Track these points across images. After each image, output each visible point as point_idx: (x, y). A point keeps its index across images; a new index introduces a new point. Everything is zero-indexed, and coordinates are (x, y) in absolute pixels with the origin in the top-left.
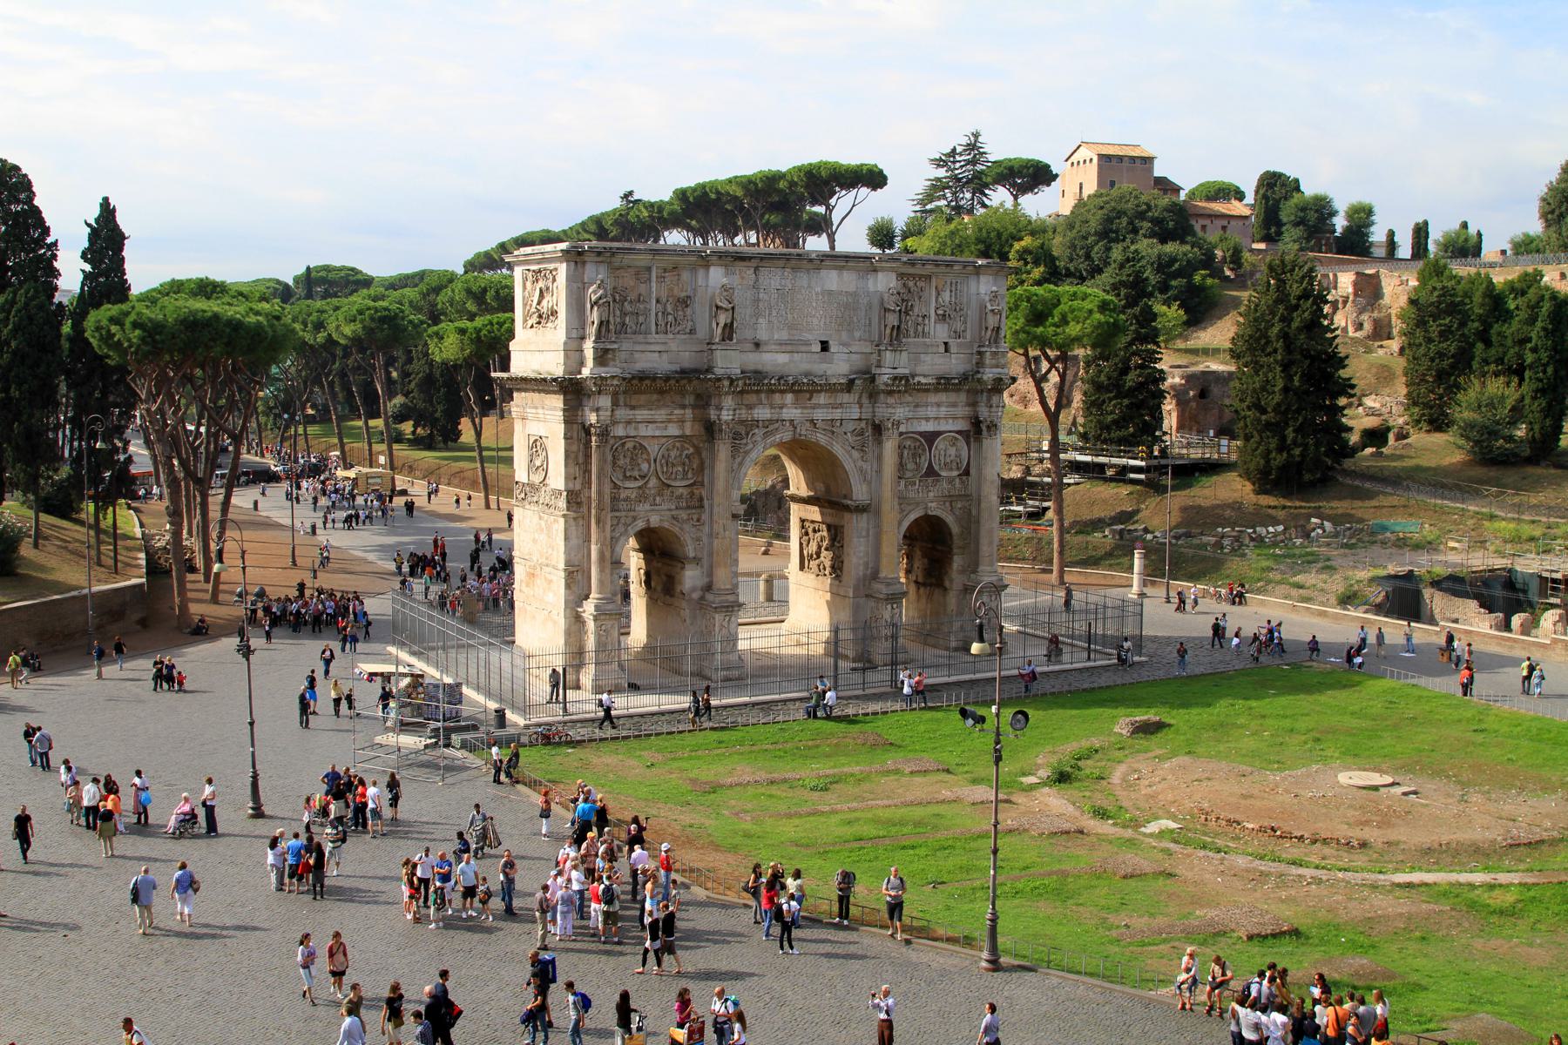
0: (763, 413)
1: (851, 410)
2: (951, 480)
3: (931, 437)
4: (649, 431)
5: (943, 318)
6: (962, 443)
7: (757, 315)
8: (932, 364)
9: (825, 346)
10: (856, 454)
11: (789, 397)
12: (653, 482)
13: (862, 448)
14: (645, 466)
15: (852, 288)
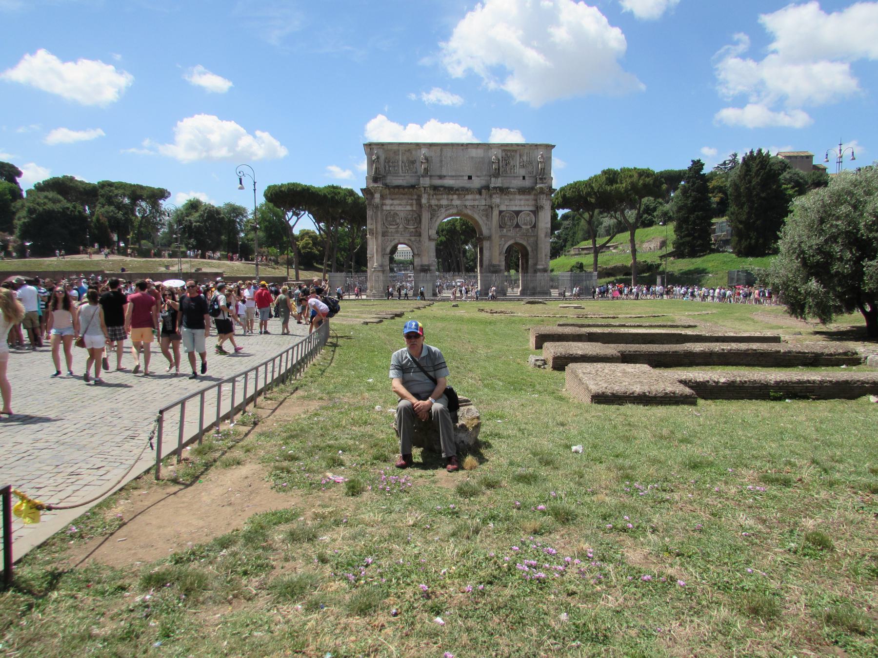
0: (444, 202)
1: (482, 202)
2: (527, 230)
3: (517, 213)
5: (523, 166)
6: (532, 215)
7: (441, 167)
8: (517, 183)
9: (470, 178)
10: (484, 218)
11: (455, 197)
12: (401, 226)
13: (487, 216)
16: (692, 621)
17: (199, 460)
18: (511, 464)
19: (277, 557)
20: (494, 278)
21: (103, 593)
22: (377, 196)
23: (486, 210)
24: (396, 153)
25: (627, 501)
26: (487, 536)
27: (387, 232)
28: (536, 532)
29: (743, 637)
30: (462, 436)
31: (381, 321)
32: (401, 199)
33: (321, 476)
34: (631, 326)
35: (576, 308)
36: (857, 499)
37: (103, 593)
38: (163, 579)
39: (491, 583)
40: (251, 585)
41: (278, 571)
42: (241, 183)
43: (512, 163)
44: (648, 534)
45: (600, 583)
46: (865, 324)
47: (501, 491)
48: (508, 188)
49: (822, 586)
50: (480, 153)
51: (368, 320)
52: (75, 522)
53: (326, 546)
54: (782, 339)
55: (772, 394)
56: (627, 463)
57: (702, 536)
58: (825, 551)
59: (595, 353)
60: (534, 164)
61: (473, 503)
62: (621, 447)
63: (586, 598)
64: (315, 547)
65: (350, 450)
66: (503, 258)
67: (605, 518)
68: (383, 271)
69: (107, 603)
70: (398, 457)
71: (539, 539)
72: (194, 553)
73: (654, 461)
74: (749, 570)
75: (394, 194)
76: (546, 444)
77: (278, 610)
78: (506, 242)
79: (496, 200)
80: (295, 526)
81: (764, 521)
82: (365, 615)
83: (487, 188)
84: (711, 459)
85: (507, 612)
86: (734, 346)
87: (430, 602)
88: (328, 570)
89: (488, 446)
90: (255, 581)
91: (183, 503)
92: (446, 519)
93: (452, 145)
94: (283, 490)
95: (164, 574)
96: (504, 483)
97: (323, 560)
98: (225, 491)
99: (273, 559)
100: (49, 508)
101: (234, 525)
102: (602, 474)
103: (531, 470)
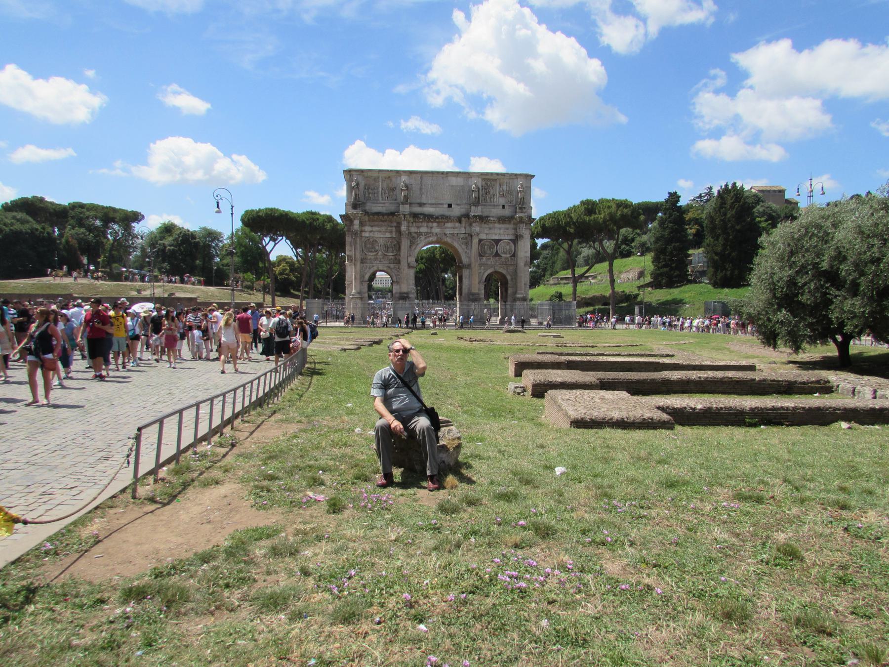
0: (424, 230)
1: (461, 230)
2: (507, 259)
3: (497, 242)
4: (379, 235)
5: (503, 196)
7: (421, 194)
8: (497, 212)
9: (450, 206)
10: (464, 247)
11: (435, 224)
12: (380, 253)
13: (467, 244)
14: (377, 248)
15: (462, 184)
16: (668, 626)
17: (175, 480)
18: (492, 483)
19: (259, 571)
20: (473, 307)
21: (81, 606)
22: (356, 222)
23: (466, 238)
24: (376, 179)
25: (605, 516)
26: (469, 550)
27: (366, 259)
28: (516, 546)
29: (717, 640)
30: (443, 456)
31: (359, 348)
32: (381, 226)
33: (301, 495)
34: (609, 355)
35: (554, 337)
36: (826, 514)
37: (81, 606)
38: (143, 592)
39: (473, 593)
40: (234, 597)
41: (260, 584)
42: (218, 207)
43: (492, 192)
44: (627, 547)
45: (580, 592)
46: (837, 354)
47: (481, 508)
48: (487, 217)
49: (792, 593)
50: (460, 181)
51: (346, 347)
52: (50, 539)
53: (307, 559)
54: (757, 367)
55: (747, 420)
56: (606, 482)
57: (678, 548)
58: (795, 561)
59: (574, 381)
60: (514, 194)
61: (454, 520)
62: (599, 468)
63: (566, 605)
64: (297, 561)
65: (330, 470)
66: (482, 287)
67: (584, 532)
68: (362, 299)
69: (86, 616)
70: (379, 478)
71: (520, 553)
72: (174, 567)
73: (632, 481)
74: (723, 579)
75: (374, 221)
76: (526, 465)
77: (261, 620)
78: (485, 270)
79: (476, 228)
80: (277, 541)
81: (737, 535)
82: (349, 623)
83: (467, 216)
84: (687, 478)
85: (489, 620)
86: (710, 374)
87: (413, 611)
88: (311, 582)
89: (469, 466)
90: (237, 593)
91: (161, 521)
92: (428, 535)
93: (432, 173)
94: (263, 507)
95: (144, 587)
96: (484, 501)
97: (306, 573)
98: (204, 509)
99: (254, 571)
100: (25, 522)
101: (214, 541)
102: (581, 492)
103: (511, 489)
